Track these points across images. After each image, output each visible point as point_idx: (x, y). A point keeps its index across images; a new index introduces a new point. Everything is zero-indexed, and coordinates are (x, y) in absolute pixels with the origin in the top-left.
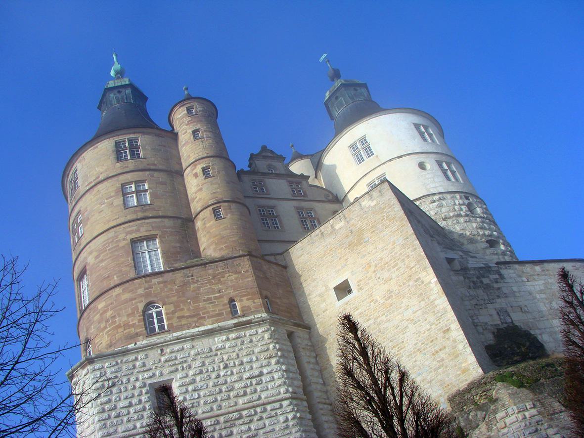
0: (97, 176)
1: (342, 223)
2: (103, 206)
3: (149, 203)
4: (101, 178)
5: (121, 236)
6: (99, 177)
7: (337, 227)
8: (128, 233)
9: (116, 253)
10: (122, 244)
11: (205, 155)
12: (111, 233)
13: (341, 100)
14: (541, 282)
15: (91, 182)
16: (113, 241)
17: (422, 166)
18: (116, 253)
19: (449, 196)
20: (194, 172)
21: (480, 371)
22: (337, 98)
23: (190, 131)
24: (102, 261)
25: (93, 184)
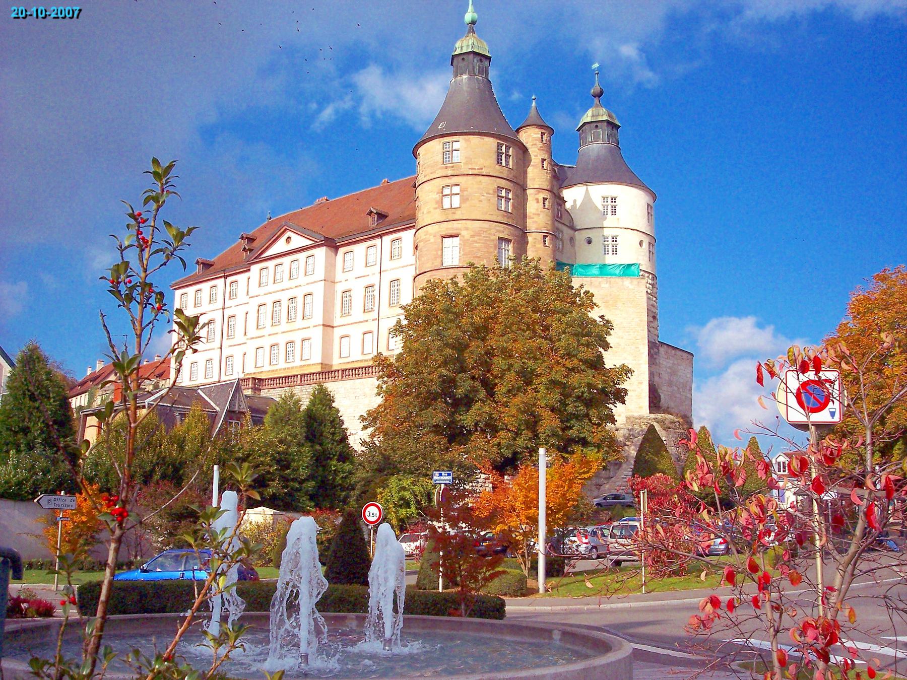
0: (480, 167)
1: (607, 286)
2: (483, 197)
3: (510, 211)
4: (484, 172)
5: (493, 231)
6: (482, 169)
7: (603, 285)
8: (499, 231)
9: (488, 243)
10: (493, 237)
11: (545, 188)
12: (486, 225)
13: (598, 134)
14: (671, 362)
15: (474, 169)
16: (486, 232)
17: (641, 243)
18: (488, 243)
19: (646, 275)
20: (537, 196)
21: (648, 411)
22: (597, 126)
23: (540, 157)
24: (476, 242)
25: (476, 172)
